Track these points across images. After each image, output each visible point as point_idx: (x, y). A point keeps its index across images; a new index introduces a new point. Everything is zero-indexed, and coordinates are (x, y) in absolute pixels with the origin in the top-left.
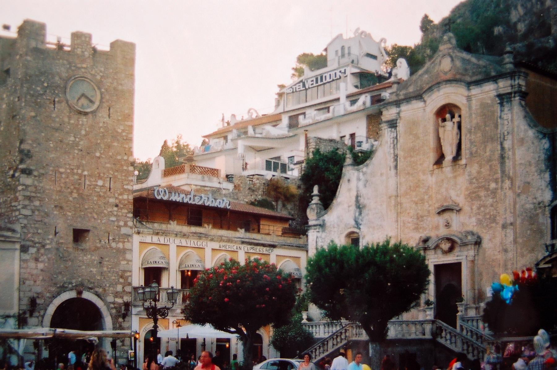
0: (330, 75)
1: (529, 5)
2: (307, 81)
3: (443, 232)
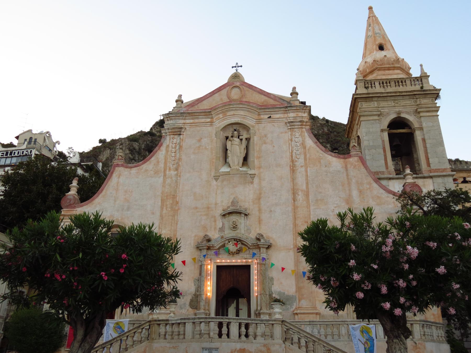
0: (19, 152)
3: (229, 234)
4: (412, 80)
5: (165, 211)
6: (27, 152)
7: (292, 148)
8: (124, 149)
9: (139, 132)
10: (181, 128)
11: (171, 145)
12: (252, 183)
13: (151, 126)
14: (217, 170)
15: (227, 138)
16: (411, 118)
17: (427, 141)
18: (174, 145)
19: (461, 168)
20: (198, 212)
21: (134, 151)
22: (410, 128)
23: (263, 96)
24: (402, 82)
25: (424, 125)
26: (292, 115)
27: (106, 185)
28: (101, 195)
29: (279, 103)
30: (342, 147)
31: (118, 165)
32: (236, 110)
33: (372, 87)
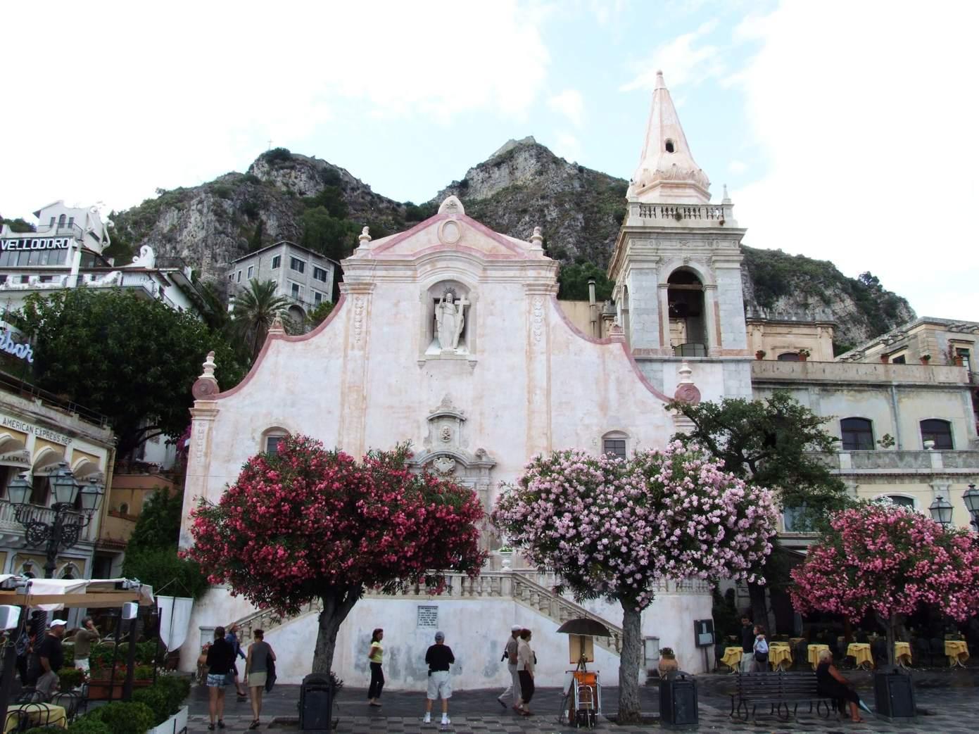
0: (43, 242)
1: (162, 252)
2: (5, 242)
3: (438, 447)
4: (709, 208)
5: (347, 411)
6: (58, 244)
7: (531, 324)
8: (205, 210)
9: (229, 174)
10: (371, 284)
11: (353, 309)
12: (471, 373)
13: (252, 161)
14: (422, 352)
15: (437, 301)
16: (702, 269)
17: (721, 307)
18: (359, 310)
19: (779, 319)
20: (394, 413)
21: (225, 216)
22: (700, 283)
23: (491, 240)
24: (694, 210)
25: (719, 282)
26: (531, 273)
27: (258, 366)
28: (251, 382)
29: (514, 253)
30: (605, 222)
31: (275, 337)
32: (450, 260)
33: (650, 216)
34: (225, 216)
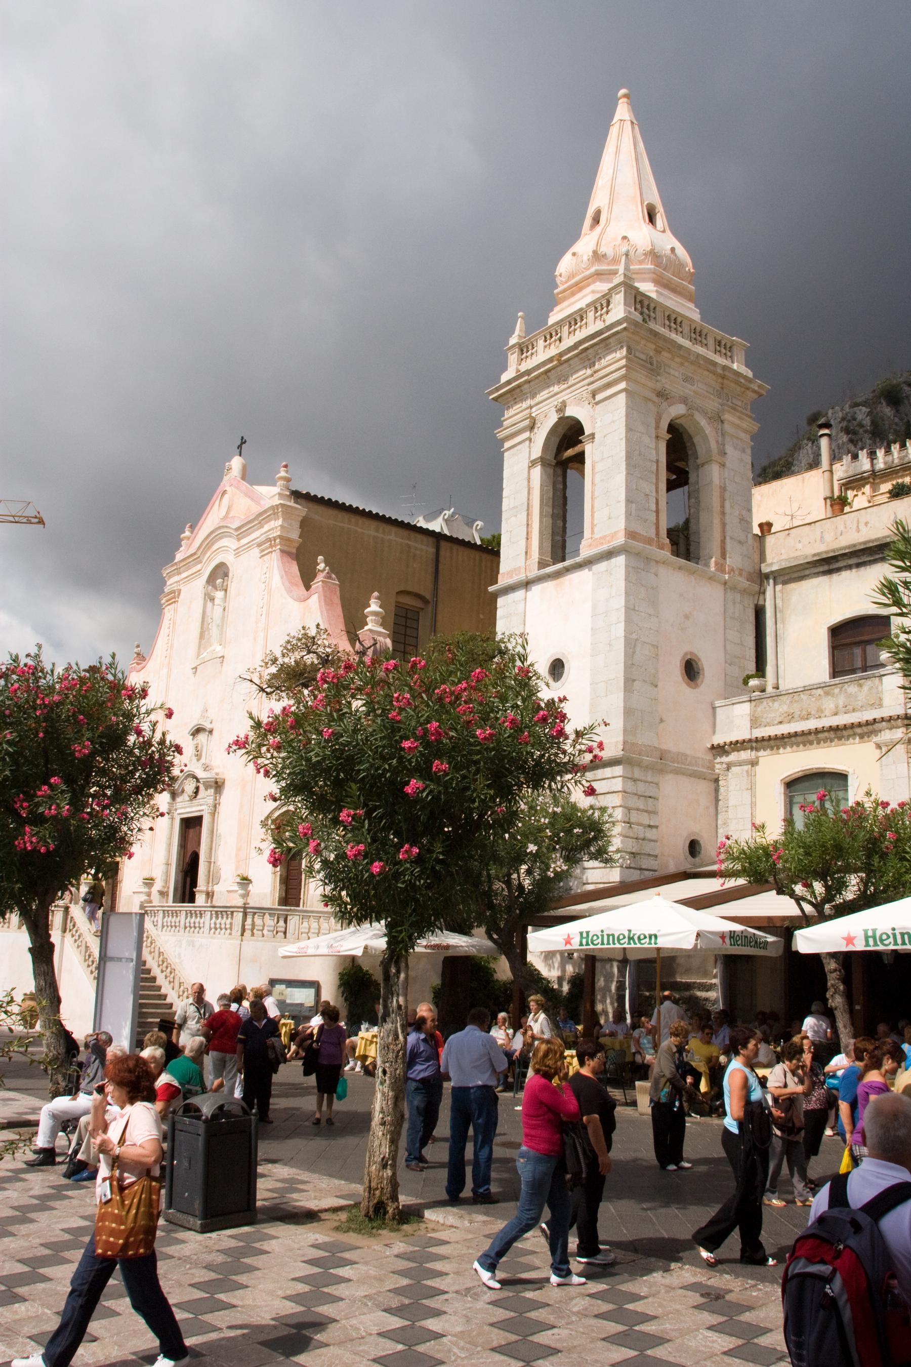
10: (174, 592)
21: (861, 431)
34: (861, 431)
